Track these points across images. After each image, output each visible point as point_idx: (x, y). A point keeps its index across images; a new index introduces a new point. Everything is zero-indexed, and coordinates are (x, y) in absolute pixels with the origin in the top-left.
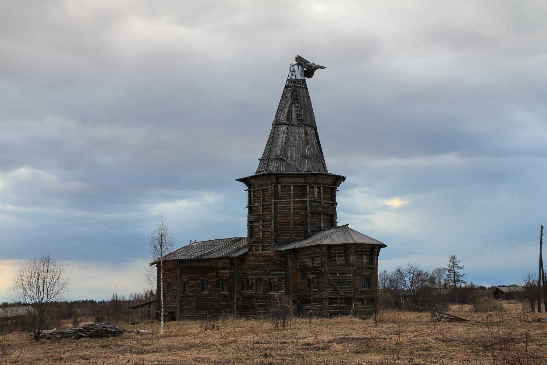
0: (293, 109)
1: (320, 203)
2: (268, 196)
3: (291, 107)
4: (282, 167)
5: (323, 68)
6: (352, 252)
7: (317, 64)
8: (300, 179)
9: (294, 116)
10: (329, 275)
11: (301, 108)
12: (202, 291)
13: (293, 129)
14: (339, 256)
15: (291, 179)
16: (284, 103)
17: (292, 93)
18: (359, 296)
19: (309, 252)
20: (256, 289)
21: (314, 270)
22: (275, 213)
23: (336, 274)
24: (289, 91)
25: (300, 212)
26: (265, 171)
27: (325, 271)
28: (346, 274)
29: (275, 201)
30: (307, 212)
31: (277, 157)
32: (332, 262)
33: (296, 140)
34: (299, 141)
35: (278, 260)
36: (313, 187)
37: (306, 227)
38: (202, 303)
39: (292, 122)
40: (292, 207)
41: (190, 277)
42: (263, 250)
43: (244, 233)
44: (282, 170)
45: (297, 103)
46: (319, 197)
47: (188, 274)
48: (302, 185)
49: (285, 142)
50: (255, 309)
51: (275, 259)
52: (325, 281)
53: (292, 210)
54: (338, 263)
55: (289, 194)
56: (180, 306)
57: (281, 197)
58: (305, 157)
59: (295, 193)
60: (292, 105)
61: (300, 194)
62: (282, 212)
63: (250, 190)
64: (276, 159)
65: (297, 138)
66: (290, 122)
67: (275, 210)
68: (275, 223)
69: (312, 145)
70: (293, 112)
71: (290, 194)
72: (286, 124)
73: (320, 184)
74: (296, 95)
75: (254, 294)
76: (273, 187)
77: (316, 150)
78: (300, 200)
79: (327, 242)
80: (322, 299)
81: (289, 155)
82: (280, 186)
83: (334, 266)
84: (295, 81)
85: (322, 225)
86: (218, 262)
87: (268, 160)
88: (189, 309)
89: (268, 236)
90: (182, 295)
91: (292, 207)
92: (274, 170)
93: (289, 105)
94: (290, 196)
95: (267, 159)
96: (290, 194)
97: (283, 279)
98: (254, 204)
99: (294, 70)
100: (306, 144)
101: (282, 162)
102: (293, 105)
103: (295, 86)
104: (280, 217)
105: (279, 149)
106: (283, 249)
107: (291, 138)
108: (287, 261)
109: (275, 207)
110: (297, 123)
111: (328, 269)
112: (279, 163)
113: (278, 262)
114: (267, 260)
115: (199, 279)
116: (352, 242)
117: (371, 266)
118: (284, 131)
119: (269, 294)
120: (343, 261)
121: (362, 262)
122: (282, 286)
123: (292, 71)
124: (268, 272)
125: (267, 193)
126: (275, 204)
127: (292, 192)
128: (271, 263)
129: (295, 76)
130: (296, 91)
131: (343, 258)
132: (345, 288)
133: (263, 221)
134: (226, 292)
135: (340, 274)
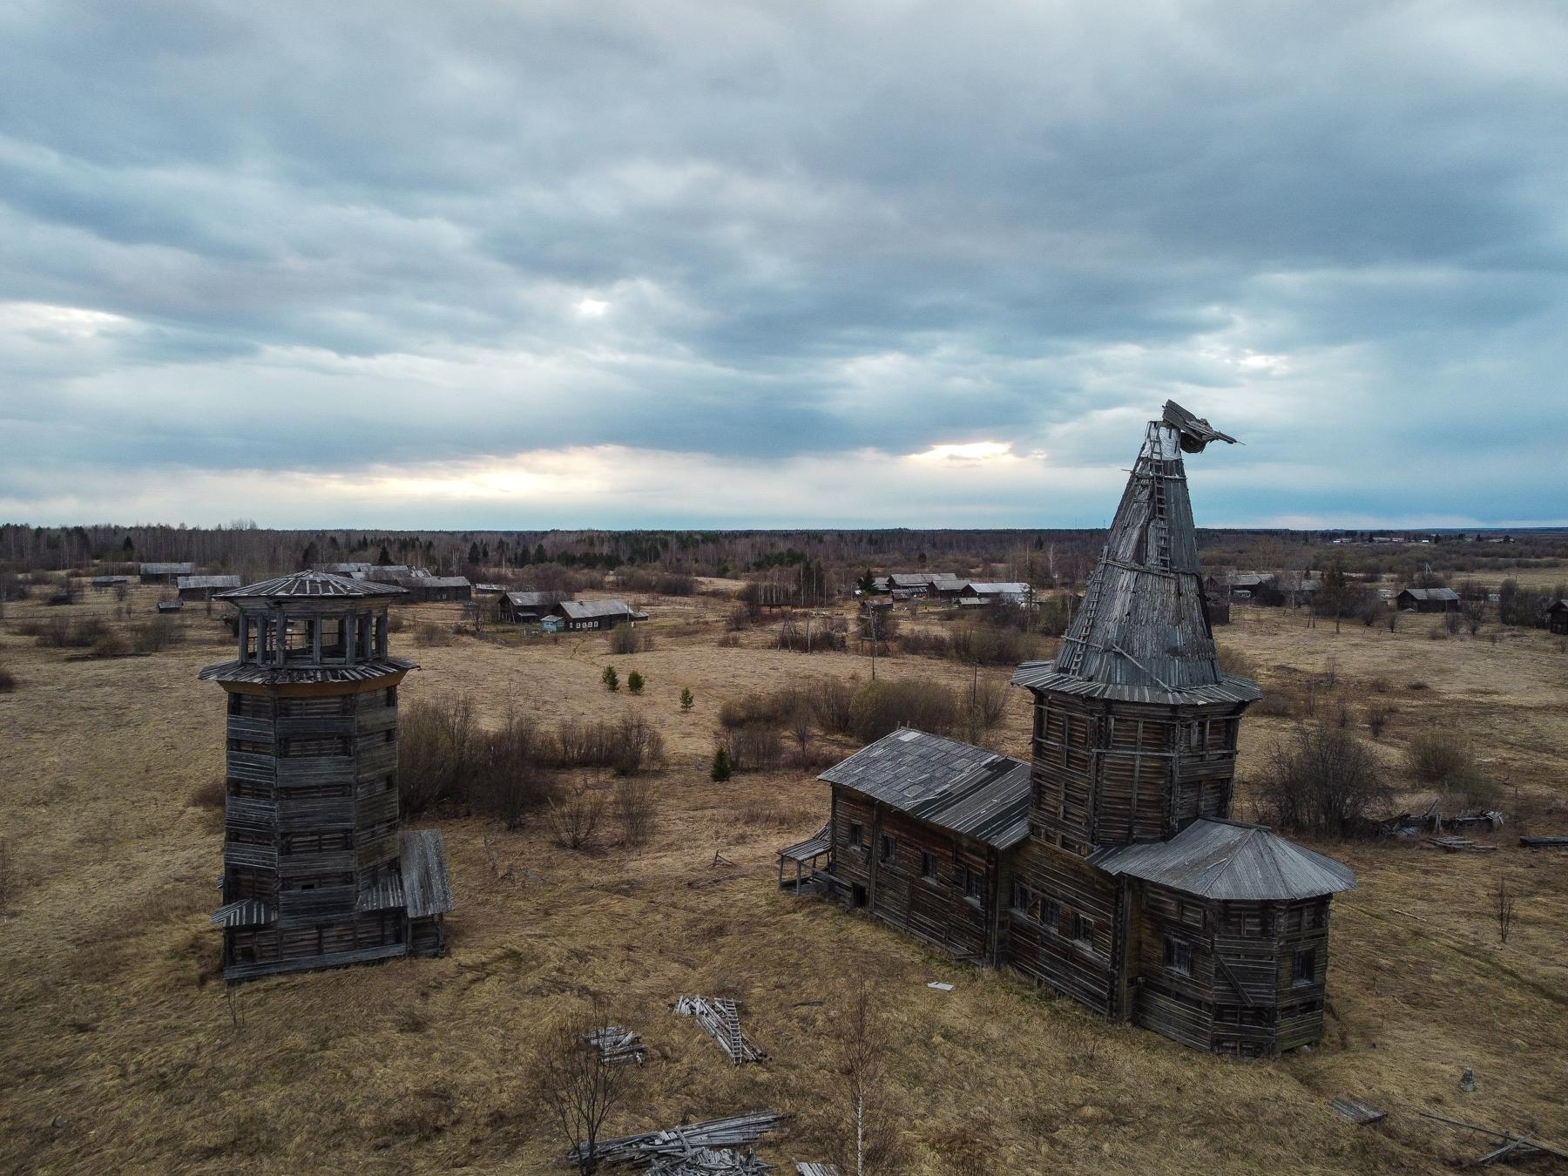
0: (1151, 532)
1: (1202, 757)
2: (1083, 733)
3: (1147, 531)
4: (1118, 673)
5: (1231, 441)
6: (1281, 910)
7: (1216, 427)
9: (1152, 551)
10: (1222, 957)
11: (1170, 532)
13: (1149, 581)
14: (1249, 916)
16: (1129, 515)
17: (1151, 495)
18: (1285, 1003)
20: (1042, 917)
21: (1185, 930)
22: (1097, 776)
23: (1239, 956)
24: (1145, 487)
25: (1158, 778)
26: (1079, 675)
27: (1213, 948)
28: (1262, 957)
30: (1171, 782)
31: (1107, 648)
32: (1230, 928)
33: (1155, 609)
34: (1161, 613)
36: (1189, 726)
37: (1166, 814)
39: (1148, 564)
40: (1137, 769)
42: (1064, 845)
44: (1118, 680)
45: (1162, 519)
46: (1202, 745)
48: (1164, 721)
49: (1129, 614)
50: (1038, 959)
53: (1137, 774)
54: (1244, 934)
55: (1132, 737)
57: (1115, 741)
58: (1174, 651)
59: (1146, 736)
60: (1148, 524)
61: (1158, 739)
62: (1116, 775)
64: (1106, 651)
65: (1158, 604)
66: (1143, 565)
67: (1098, 771)
68: (1096, 799)
69: (1191, 620)
70: (1151, 540)
71: (1136, 738)
72: (1132, 570)
73: (1205, 716)
74: (1160, 501)
76: (1096, 719)
77: (1199, 628)
78: (1157, 754)
79: (1220, 889)
80: (1199, 1003)
81: (1136, 645)
82: (1113, 721)
83: (1235, 938)
84: (1161, 466)
85: (1203, 803)
87: (1087, 647)
88: (895, 899)
89: (1078, 819)
90: (882, 865)
91: (1137, 769)
92: (1100, 677)
94: (1135, 743)
95: (1082, 645)
96: (1136, 738)
97: (1108, 927)
98: (1047, 739)
99: (1158, 437)
100: (1179, 618)
101: (1119, 661)
102: (1152, 524)
103: (1159, 478)
104: (1108, 786)
105: (1112, 628)
106: (1113, 867)
107: (1143, 605)
108: (1121, 895)
109: (1098, 764)
110: (1159, 567)
111: (1220, 943)
112: (1113, 662)
113: (1097, 887)
116: (1283, 896)
117: (1318, 931)
118: (1128, 586)
120: (1256, 925)
121: (1299, 924)
123: (1155, 442)
125: (1082, 727)
126: (1098, 757)
127: (1140, 734)
129: (1161, 454)
130: (1160, 491)
131: (1257, 920)
132: (1257, 987)
133: (1066, 785)
134: (974, 901)
135: (1246, 956)
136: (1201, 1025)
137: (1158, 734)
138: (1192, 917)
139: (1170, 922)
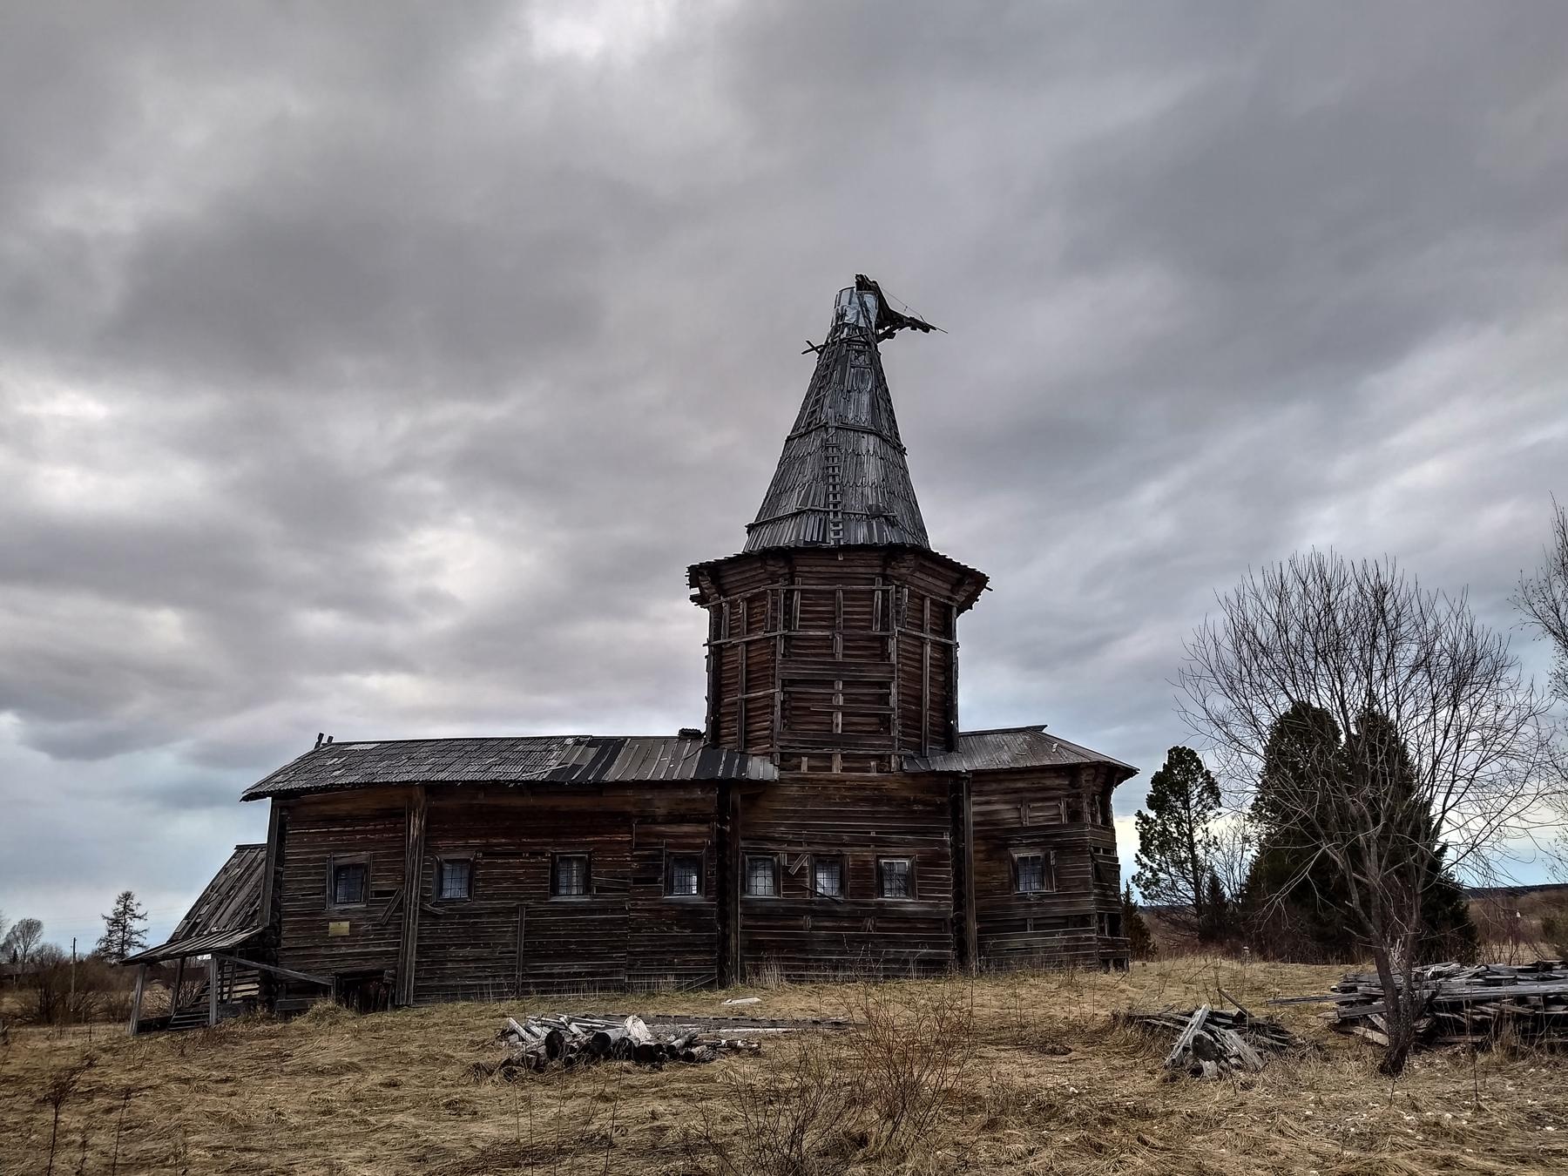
8: (945, 586)
12: (551, 896)
15: (930, 579)
19: (1020, 785)
29: (899, 629)
35: (916, 802)
38: (559, 936)
41: (487, 845)
43: (698, 721)
50: (813, 952)
51: (907, 799)
52: (1087, 867)
56: (421, 951)
63: (792, 587)
75: (810, 902)
86: (648, 797)
93: (869, 387)
97: (945, 857)
114: (865, 799)
115: (542, 854)
119: (881, 904)
124: (873, 834)
128: (886, 808)
133: (845, 683)
137: (936, 617)
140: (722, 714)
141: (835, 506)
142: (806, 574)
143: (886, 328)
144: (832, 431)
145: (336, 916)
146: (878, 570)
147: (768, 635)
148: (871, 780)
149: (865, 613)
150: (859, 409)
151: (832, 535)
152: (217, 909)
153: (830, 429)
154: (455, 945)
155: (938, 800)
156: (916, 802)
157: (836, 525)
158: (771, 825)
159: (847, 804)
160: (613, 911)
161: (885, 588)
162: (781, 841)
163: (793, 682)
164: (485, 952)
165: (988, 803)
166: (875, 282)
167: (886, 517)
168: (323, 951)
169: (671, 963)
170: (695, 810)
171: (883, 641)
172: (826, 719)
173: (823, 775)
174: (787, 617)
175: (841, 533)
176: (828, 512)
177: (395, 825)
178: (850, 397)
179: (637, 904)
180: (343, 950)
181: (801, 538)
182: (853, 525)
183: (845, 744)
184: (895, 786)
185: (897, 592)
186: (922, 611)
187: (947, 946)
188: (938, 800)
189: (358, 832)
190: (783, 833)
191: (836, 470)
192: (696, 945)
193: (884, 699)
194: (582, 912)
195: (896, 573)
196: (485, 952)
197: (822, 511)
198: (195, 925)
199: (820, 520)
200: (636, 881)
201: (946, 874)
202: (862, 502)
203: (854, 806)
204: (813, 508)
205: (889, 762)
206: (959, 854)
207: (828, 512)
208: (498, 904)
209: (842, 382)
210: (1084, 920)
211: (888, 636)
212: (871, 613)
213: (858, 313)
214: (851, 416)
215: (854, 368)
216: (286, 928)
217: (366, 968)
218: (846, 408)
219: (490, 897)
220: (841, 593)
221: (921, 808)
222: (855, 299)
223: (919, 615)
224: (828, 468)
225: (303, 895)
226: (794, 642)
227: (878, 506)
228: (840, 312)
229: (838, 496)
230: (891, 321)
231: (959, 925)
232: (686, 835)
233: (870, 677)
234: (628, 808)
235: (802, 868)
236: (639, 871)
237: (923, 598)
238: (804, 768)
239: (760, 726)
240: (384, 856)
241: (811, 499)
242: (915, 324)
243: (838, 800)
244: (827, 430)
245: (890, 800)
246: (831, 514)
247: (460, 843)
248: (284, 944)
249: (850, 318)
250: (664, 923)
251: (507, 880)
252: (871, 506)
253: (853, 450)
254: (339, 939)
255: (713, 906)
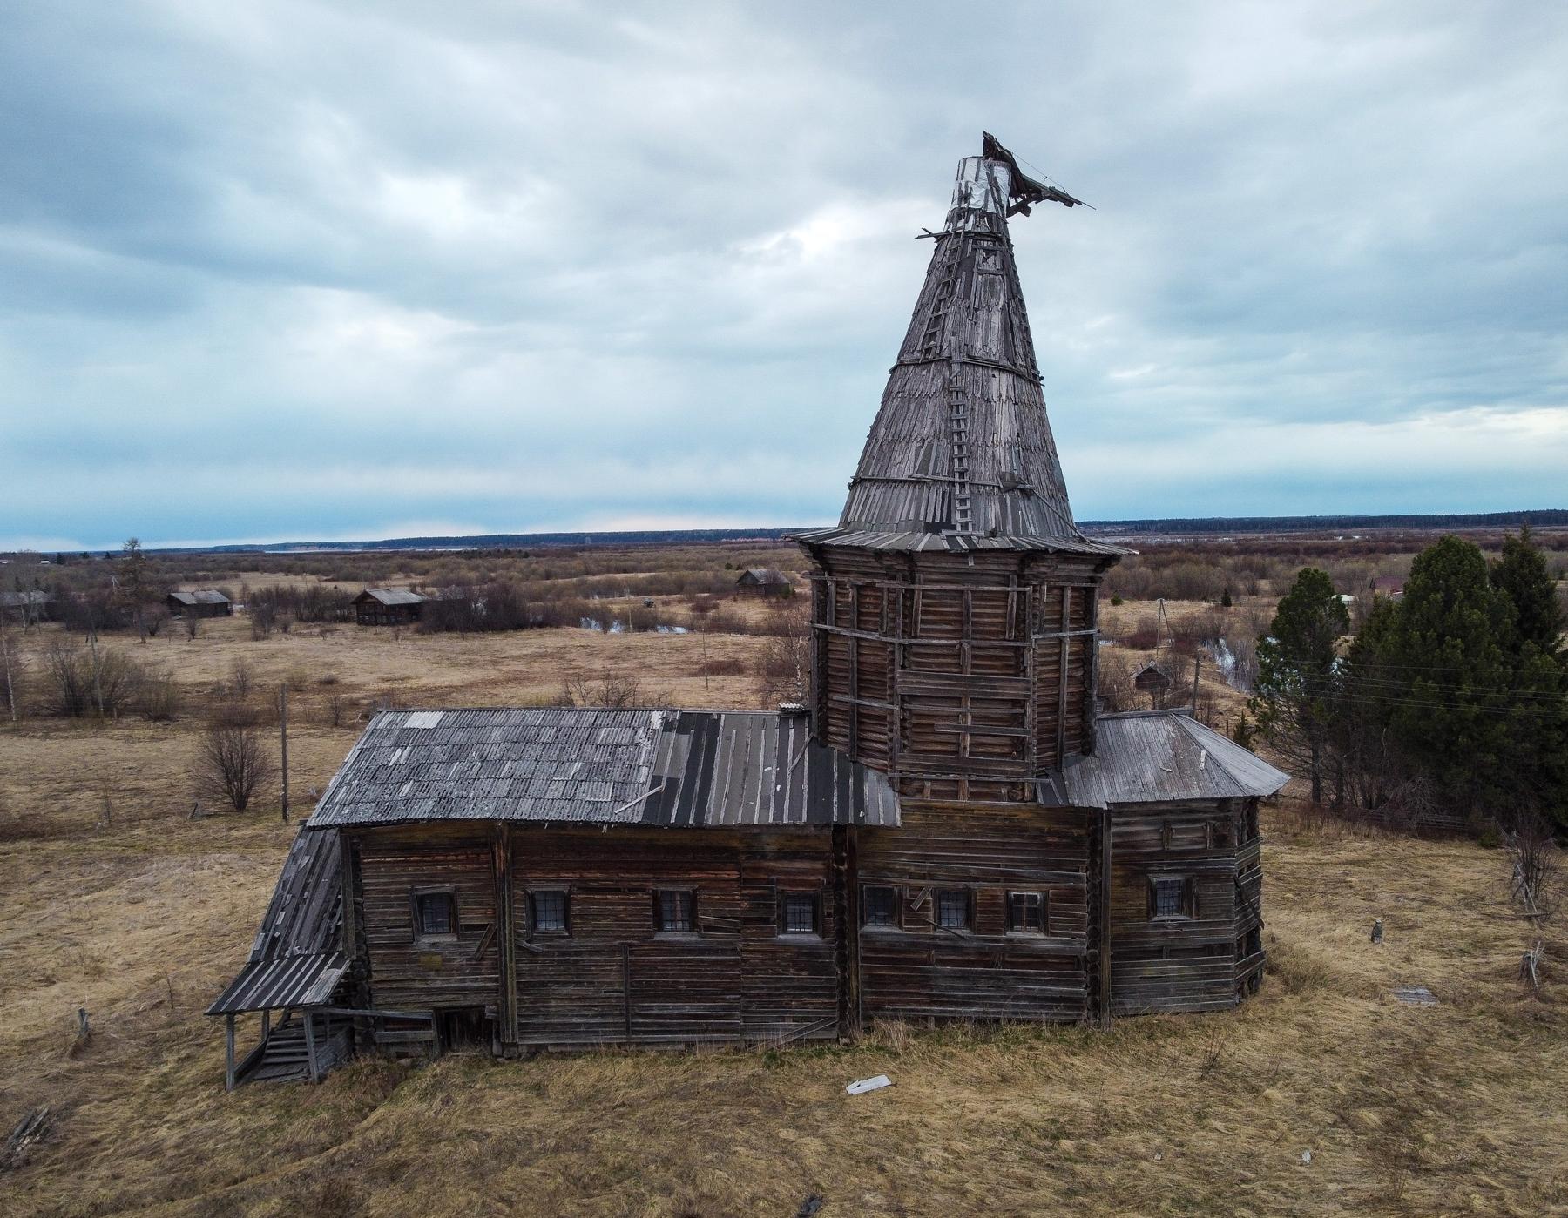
35: (1050, 833)
38: (667, 976)
41: (581, 880)
47: (567, 870)
50: (938, 987)
51: (1040, 830)
97: (1080, 892)
114: (996, 829)
115: (643, 890)
119: (1010, 940)
122: (1074, 915)
128: (1017, 840)
134: (800, 936)
136: (1219, 976)
138: (1184, 839)
139: (1151, 855)
140: (828, 708)
141: (962, 474)
142: (929, 570)
143: (1020, 200)
144: (956, 369)
145: (427, 949)
146: (1013, 568)
147: (884, 639)
148: (1003, 809)
149: (996, 616)
150: (988, 338)
151: (958, 515)
152: (294, 917)
153: (953, 365)
154: (557, 983)
155: (1076, 832)
156: (1050, 833)
157: (963, 501)
158: (890, 856)
159: (974, 835)
160: (724, 952)
161: (1021, 589)
162: (902, 874)
163: (913, 698)
164: (591, 992)
165: (1125, 824)
166: (1009, 152)
167: (1022, 491)
168: (418, 985)
169: (788, 1004)
170: (808, 846)
171: (1019, 652)
172: (953, 739)
173: (948, 802)
174: (907, 621)
175: (969, 513)
176: (953, 483)
177: (478, 855)
178: (977, 317)
179: (749, 945)
180: (438, 985)
181: (922, 518)
182: (981, 501)
183: (974, 770)
184: (1027, 816)
185: (1035, 591)
186: (1061, 602)
187: (1079, 984)
188: (1076, 832)
189: (438, 862)
190: (904, 865)
191: (962, 423)
192: (815, 988)
193: (1018, 720)
194: (690, 951)
195: (1035, 571)
196: (591, 992)
197: (945, 481)
198: (274, 941)
199: (944, 493)
200: (747, 920)
201: (1082, 910)
202: (993, 469)
203: (982, 836)
204: (936, 477)
205: (1023, 790)
206: (1097, 891)
207: (953, 483)
208: (599, 941)
209: (967, 296)
210: (1223, 948)
211: (1024, 648)
212: (1004, 616)
213: (987, 191)
214: (979, 345)
215: (982, 274)
216: (375, 960)
217: (463, 1004)
218: (972, 334)
219: (590, 934)
220: (970, 595)
221: (1056, 840)
222: (983, 174)
223: (1057, 608)
224: (951, 420)
225: (388, 928)
226: (915, 650)
227: (1012, 475)
228: (963, 188)
229: (965, 460)
230: (1027, 192)
231: (1093, 964)
232: (800, 872)
233: (1003, 694)
234: (735, 843)
235: (926, 902)
236: (750, 910)
237: (1062, 589)
238: (927, 793)
239: (877, 737)
240: (471, 889)
241: (932, 464)
242: (1055, 195)
243: (965, 831)
244: (950, 366)
245: (1023, 831)
246: (957, 487)
247: (552, 876)
248: (376, 977)
249: (976, 201)
250: (778, 965)
251: (606, 917)
252: (1005, 473)
253: (982, 395)
254: (432, 973)
255: (831, 948)
